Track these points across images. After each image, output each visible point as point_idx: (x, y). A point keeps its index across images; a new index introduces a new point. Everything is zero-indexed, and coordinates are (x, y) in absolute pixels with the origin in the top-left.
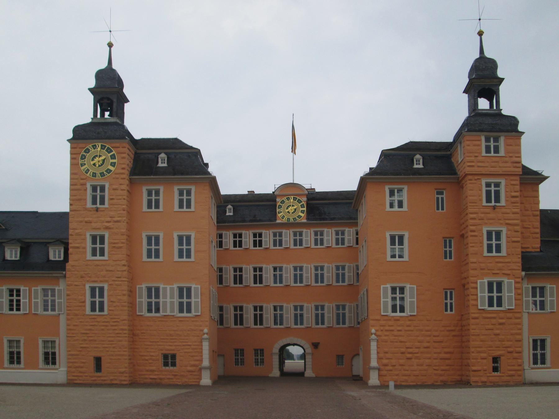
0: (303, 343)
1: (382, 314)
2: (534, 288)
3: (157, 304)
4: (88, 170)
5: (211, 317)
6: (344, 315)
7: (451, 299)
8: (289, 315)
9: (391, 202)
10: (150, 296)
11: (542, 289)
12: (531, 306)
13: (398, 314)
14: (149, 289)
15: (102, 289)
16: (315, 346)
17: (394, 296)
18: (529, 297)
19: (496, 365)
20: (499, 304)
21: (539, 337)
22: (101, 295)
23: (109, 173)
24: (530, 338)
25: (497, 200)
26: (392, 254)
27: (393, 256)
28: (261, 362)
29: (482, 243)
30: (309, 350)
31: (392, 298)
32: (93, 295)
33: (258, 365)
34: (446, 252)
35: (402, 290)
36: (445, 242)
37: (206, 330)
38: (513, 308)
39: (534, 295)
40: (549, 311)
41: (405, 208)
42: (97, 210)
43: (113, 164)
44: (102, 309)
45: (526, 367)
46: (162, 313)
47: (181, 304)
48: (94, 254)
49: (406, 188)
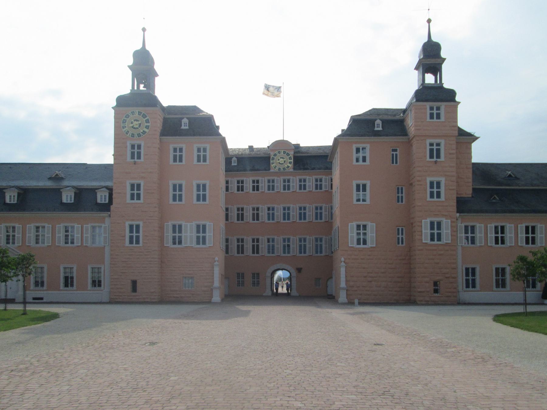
0: (289, 268)
1: (350, 245)
2: (466, 227)
3: (180, 238)
4: (128, 132)
5: (221, 247)
6: (321, 246)
7: (402, 234)
8: (279, 246)
9: (357, 157)
10: (174, 231)
11: (473, 227)
12: (464, 241)
13: (362, 246)
14: (174, 226)
15: (138, 227)
16: (299, 270)
17: (359, 231)
18: (462, 233)
19: (436, 288)
20: (439, 239)
21: (470, 266)
22: (138, 231)
23: (144, 134)
24: (463, 267)
25: (438, 156)
26: (358, 198)
27: (358, 200)
28: (257, 284)
29: (426, 190)
30: (294, 274)
31: (357, 233)
32: (131, 231)
33: (255, 286)
34: (398, 197)
35: (365, 227)
36: (398, 189)
37: (217, 259)
38: (450, 242)
39: (466, 232)
40: (478, 245)
41: (368, 162)
42: (135, 163)
43: (147, 127)
44: (138, 242)
45: (460, 288)
46: (183, 245)
47: (198, 238)
48: (132, 198)
49: (368, 146)
